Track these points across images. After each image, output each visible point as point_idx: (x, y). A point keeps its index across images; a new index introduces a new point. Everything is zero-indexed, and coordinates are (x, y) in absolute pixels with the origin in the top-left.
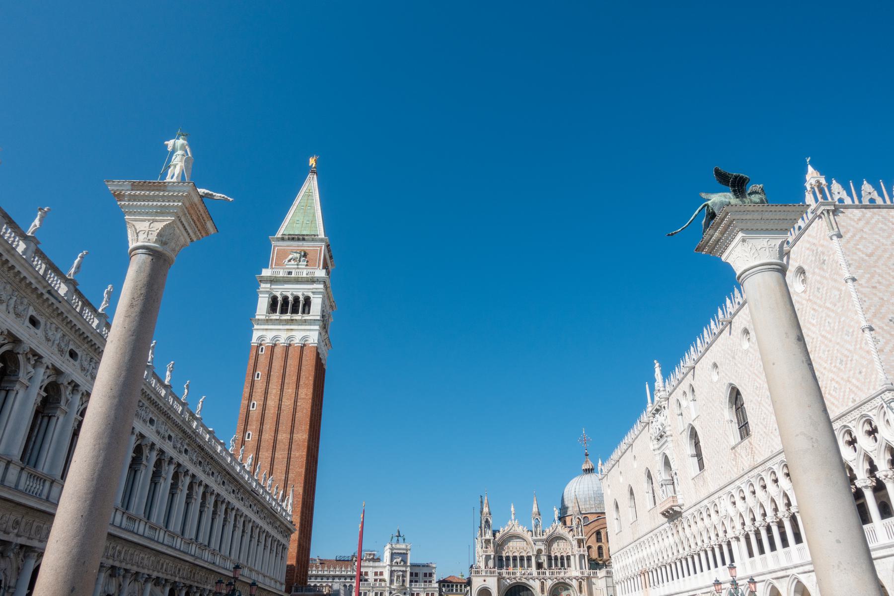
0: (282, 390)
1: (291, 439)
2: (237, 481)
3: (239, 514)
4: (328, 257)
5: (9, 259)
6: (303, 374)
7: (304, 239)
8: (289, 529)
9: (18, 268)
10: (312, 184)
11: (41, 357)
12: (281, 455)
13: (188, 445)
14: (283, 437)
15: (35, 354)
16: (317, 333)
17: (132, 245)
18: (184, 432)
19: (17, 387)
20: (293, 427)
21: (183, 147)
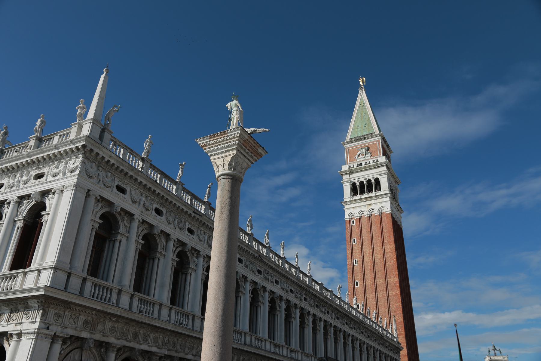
0: (373, 248)
1: (387, 282)
2: (348, 316)
3: (354, 339)
4: (385, 146)
5: (168, 198)
6: (385, 234)
7: (365, 138)
8: (398, 348)
9: (174, 202)
10: (362, 96)
11: (199, 251)
12: (382, 294)
13: (306, 295)
14: (381, 281)
15: (196, 250)
16: (389, 203)
17: (217, 175)
18: (300, 287)
19: (190, 271)
20: (386, 273)
21: (236, 105)
